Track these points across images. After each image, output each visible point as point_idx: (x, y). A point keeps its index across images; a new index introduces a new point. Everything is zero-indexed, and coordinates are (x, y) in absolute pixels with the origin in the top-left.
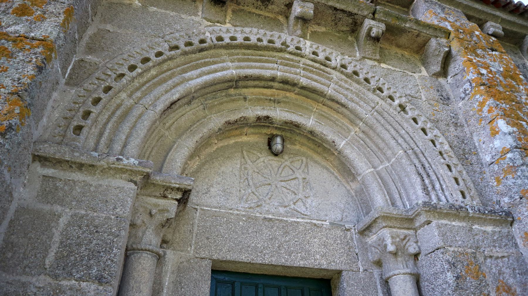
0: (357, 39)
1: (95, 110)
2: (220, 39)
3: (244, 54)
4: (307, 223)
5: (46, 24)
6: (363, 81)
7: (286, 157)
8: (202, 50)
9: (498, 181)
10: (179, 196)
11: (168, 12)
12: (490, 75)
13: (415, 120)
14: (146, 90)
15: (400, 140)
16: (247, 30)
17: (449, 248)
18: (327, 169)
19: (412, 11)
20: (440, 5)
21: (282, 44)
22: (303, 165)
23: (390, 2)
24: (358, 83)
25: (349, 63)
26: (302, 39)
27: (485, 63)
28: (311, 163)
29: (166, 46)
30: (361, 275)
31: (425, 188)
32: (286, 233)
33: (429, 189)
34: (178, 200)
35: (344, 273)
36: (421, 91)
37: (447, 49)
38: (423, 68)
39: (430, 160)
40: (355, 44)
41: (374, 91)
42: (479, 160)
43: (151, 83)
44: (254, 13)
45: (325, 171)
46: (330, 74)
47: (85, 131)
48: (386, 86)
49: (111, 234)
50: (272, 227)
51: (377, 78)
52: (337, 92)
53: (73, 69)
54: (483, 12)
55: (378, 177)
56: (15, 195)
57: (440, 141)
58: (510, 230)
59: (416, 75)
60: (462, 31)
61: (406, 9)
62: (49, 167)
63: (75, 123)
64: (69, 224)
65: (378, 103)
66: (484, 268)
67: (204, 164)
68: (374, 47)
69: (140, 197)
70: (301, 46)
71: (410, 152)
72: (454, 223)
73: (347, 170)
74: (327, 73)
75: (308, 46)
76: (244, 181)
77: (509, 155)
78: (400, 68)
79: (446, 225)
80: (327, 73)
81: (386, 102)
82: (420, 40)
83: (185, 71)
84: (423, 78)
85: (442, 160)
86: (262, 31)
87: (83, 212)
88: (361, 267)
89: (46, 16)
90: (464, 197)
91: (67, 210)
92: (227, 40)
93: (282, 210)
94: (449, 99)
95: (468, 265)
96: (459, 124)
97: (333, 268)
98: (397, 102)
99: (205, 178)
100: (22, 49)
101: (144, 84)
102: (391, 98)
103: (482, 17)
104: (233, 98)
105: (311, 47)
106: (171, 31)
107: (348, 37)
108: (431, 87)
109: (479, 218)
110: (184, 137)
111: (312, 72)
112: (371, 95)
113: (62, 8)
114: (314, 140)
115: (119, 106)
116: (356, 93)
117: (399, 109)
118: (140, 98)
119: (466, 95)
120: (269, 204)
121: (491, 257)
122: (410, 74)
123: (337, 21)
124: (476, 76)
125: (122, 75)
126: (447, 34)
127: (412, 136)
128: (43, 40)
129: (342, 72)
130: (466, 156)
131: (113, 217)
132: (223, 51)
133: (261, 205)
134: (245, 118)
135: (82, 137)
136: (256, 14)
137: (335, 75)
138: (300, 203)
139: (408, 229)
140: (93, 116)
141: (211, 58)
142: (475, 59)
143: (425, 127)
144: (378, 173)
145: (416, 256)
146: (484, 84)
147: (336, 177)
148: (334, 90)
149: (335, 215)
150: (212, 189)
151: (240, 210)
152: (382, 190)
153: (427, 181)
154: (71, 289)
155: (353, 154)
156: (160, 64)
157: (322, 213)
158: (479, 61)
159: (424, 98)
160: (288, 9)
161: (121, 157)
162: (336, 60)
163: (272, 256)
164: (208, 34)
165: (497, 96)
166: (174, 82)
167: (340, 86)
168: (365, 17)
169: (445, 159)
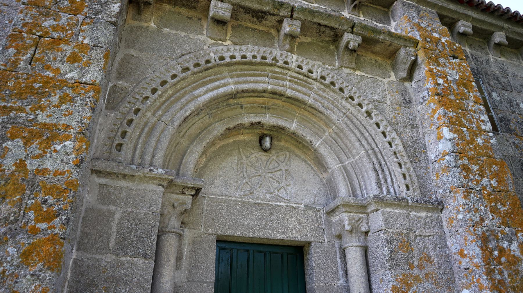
0: (337, 47)
1: (130, 130)
2: (222, 58)
3: (241, 70)
4: (287, 206)
5: (92, 69)
6: (338, 90)
7: (273, 152)
8: (207, 69)
9: (438, 176)
10: (193, 193)
11: (178, 32)
12: (446, 85)
13: (378, 125)
14: (165, 108)
15: (364, 142)
16: (244, 47)
17: (389, 230)
18: (305, 161)
19: (392, 12)
20: (416, 8)
21: (273, 60)
22: (287, 158)
23: (372, 4)
24: (334, 91)
25: (328, 75)
26: (289, 54)
27: (444, 72)
28: (293, 157)
29: (179, 68)
30: (326, 245)
31: (379, 183)
32: (271, 214)
33: (382, 182)
34: (193, 196)
35: (313, 244)
36: (388, 95)
37: (413, 58)
38: (392, 73)
39: (386, 158)
40: (336, 53)
41: (347, 99)
42: (426, 157)
43: (169, 102)
44: (250, 28)
45: (304, 163)
46: (311, 84)
47: (124, 147)
48: (357, 95)
49: (150, 225)
50: (261, 210)
51: (350, 87)
52: (316, 100)
53: (109, 94)
54: (456, 12)
55: (344, 171)
56: (85, 200)
57: (396, 142)
58: (440, 215)
59: (384, 80)
60: (429, 40)
61: (386, 10)
62: (102, 178)
63: (117, 142)
64: (121, 219)
65: (349, 109)
66: (413, 244)
67: (209, 161)
68: (351, 57)
69: (166, 194)
70: (289, 61)
71: (370, 152)
72: (396, 211)
73: (320, 164)
74: (309, 83)
75: (294, 59)
76: (240, 174)
77: (447, 158)
78: (372, 75)
79: (390, 212)
80: (309, 83)
81: (355, 108)
82: (391, 48)
83: (194, 89)
84: (391, 83)
85: (395, 159)
86: (256, 48)
87: (130, 210)
88: (326, 239)
89: (91, 61)
90: (408, 189)
91: (119, 209)
92: (228, 60)
93: (268, 196)
94: (410, 102)
95: (401, 242)
96: (415, 126)
97: (305, 240)
98: (365, 109)
99: (211, 172)
100: (79, 94)
101: (163, 103)
102: (360, 105)
103: (455, 16)
104: (232, 107)
105: (297, 61)
106: (182, 52)
107: (330, 46)
108: (396, 92)
109: (416, 207)
110: (195, 143)
111: (296, 83)
112: (344, 103)
113: (102, 53)
114: (296, 140)
115: (146, 124)
116: (332, 101)
117: (365, 115)
118: (161, 116)
119: (424, 101)
120: (259, 191)
121: (420, 236)
122: (381, 79)
123: (321, 33)
124: (433, 86)
125: (147, 98)
126: (416, 44)
127: (374, 138)
128: (92, 84)
129: (321, 83)
130: (417, 154)
131: (150, 213)
132: (225, 69)
133: (253, 193)
134: (241, 124)
135: (123, 152)
136: (252, 29)
137: (316, 85)
138: (282, 190)
139: (362, 213)
140: (128, 134)
141: (215, 75)
142: (436, 68)
143: (385, 131)
144: (345, 168)
145: (367, 233)
146: (438, 94)
147: (312, 168)
148: (314, 99)
149: (309, 200)
150: (216, 181)
151: (237, 197)
152: (346, 181)
153: (381, 176)
154: (127, 263)
155: (325, 153)
156: (175, 85)
157: (299, 198)
158: (438, 71)
159: (389, 103)
160: (279, 24)
161: (152, 168)
162: (317, 72)
163: (260, 232)
164: (212, 55)
165: (447, 105)
166: (186, 100)
167: (319, 95)
168: (345, 31)
169: (397, 158)
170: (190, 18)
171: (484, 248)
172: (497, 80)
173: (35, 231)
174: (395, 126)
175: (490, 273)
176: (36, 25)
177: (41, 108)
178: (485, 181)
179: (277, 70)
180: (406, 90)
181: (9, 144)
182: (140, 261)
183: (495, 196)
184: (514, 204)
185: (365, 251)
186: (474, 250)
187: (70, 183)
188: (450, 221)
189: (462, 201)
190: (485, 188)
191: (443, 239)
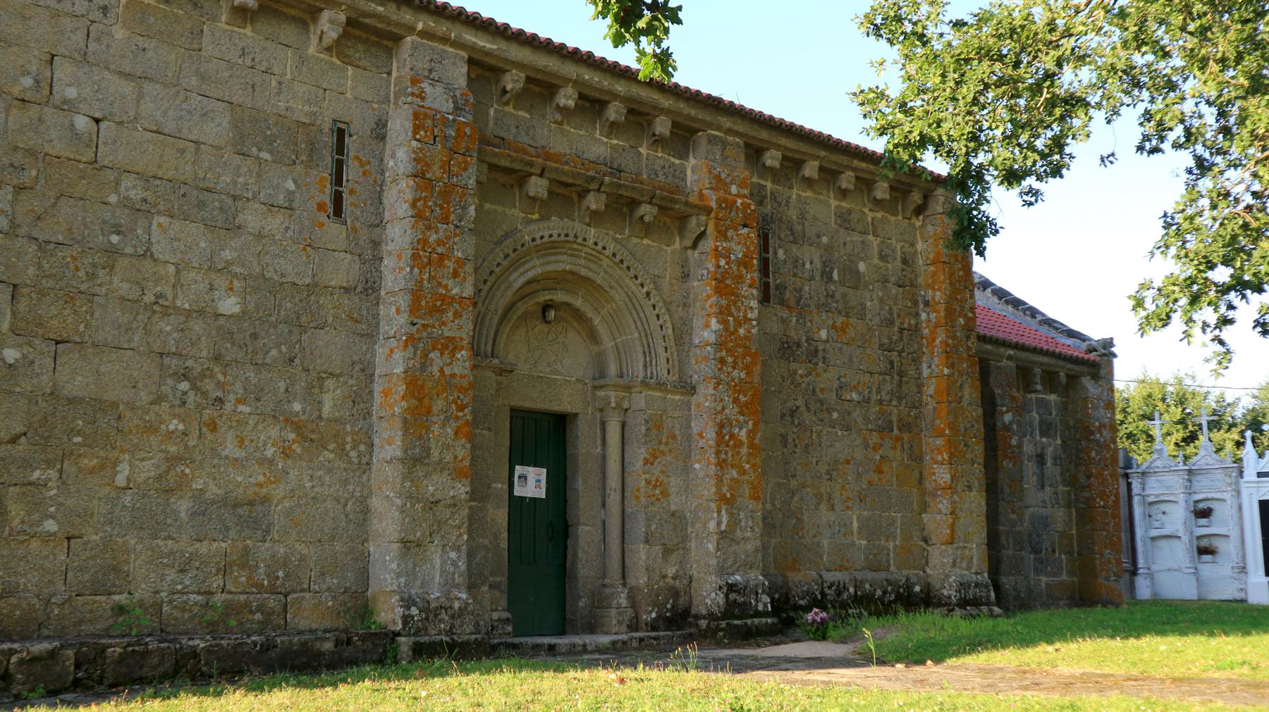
13: (654, 307)
31: (645, 366)
32: (549, 387)
59: (669, 249)
73: (593, 336)
83: (510, 274)
98: (645, 289)
112: (628, 281)
114: (578, 315)
126: (708, 211)
137: (606, 261)
170: (504, 186)
171: (719, 434)
172: (791, 230)
173: (457, 418)
174: (668, 305)
175: (718, 453)
176: (424, 242)
177: (444, 324)
178: (735, 373)
179: (575, 246)
180: (687, 260)
181: (432, 355)
183: (738, 388)
184: (754, 395)
185: (623, 425)
186: (711, 434)
187: (470, 384)
188: (698, 405)
189: (711, 391)
190: (733, 380)
191: (688, 420)
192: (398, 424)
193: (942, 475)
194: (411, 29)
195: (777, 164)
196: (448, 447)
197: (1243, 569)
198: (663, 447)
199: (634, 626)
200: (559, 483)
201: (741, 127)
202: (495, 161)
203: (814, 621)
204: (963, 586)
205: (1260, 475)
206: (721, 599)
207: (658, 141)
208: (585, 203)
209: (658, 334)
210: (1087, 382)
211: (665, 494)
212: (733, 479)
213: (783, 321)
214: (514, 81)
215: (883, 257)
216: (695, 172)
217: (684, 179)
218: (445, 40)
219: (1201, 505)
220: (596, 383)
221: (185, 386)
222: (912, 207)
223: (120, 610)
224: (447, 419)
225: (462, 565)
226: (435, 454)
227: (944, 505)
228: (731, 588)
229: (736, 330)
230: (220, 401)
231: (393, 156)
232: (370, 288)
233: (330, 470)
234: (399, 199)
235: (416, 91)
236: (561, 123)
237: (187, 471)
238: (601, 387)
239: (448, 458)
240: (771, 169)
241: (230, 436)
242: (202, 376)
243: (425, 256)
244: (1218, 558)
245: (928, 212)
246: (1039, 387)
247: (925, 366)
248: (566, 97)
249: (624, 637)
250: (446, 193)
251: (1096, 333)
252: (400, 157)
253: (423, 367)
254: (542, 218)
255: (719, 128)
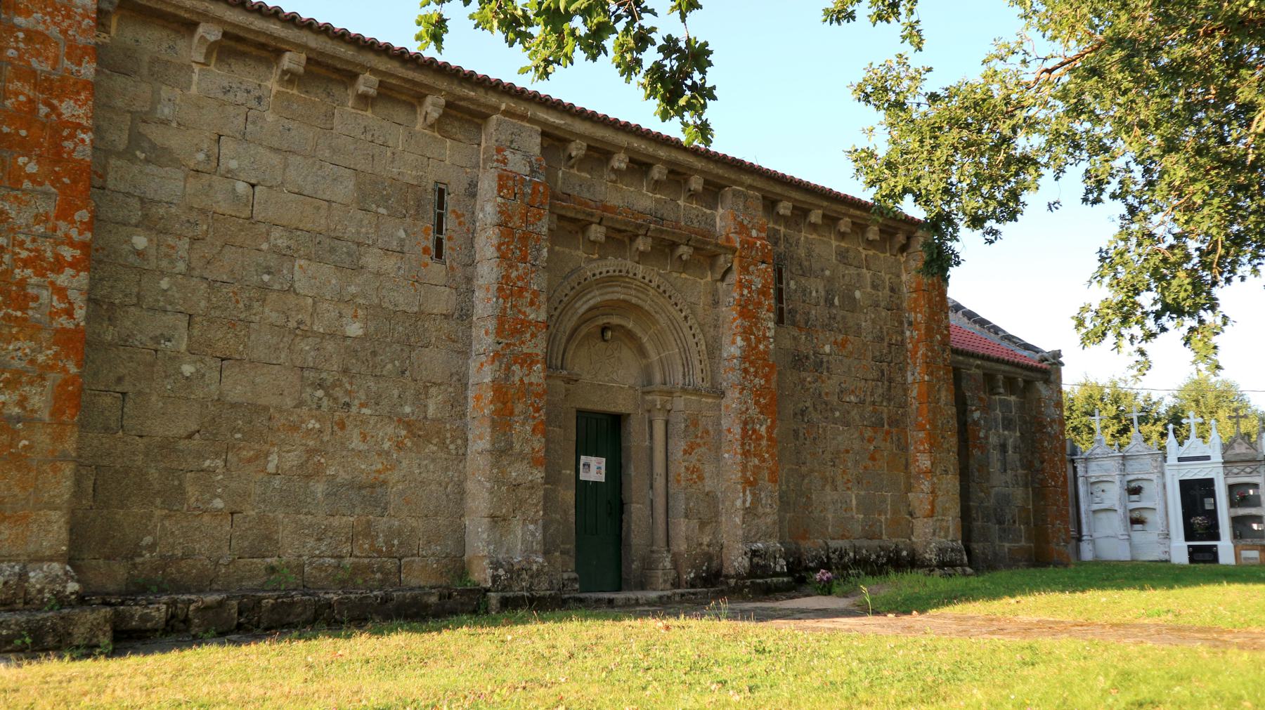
31: (684, 375)
73: (642, 352)
114: (630, 335)
126: (734, 250)
137: (652, 292)
149: (632, 382)
155: (649, 347)
171: (744, 430)
173: (534, 418)
175: (743, 444)
177: (523, 343)
178: (757, 381)
180: (716, 290)
181: (514, 368)
182: (557, 429)
183: (758, 393)
184: (771, 399)
186: (737, 430)
189: (737, 395)
191: (719, 418)
192: (487, 423)
193: (924, 462)
194: (496, 109)
195: (788, 213)
196: (527, 441)
197: (1167, 536)
198: (698, 440)
199: (676, 584)
200: (616, 470)
201: (759, 183)
202: (563, 212)
203: (821, 580)
204: (941, 551)
205: (1180, 459)
206: (746, 562)
207: (693, 195)
208: (635, 246)
209: (694, 349)
210: (1040, 386)
211: (701, 478)
212: (755, 466)
213: (795, 338)
214: (577, 149)
215: (874, 287)
216: (723, 219)
217: (714, 226)
218: (523, 117)
219: (1133, 485)
220: (645, 389)
221: (320, 393)
222: (897, 246)
223: (272, 570)
224: (526, 419)
225: (539, 535)
226: (517, 447)
227: (926, 486)
228: (755, 553)
229: (757, 346)
230: (348, 405)
231: (482, 209)
232: (464, 315)
233: (433, 460)
234: (487, 244)
235: (500, 158)
236: (615, 182)
237: (323, 460)
238: (649, 393)
239: (527, 449)
240: (784, 216)
241: (356, 431)
242: (334, 386)
243: (508, 290)
244: (1147, 527)
245: (911, 250)
246: (1002, 390)
247: (909, 374)
248: (620, 161)
249: (669, 593)
250: (525, 238)
251: (1047, 346)
252: (487, 210)
253: (507, 378)
254: (601, 258)
255: (741, 184)
